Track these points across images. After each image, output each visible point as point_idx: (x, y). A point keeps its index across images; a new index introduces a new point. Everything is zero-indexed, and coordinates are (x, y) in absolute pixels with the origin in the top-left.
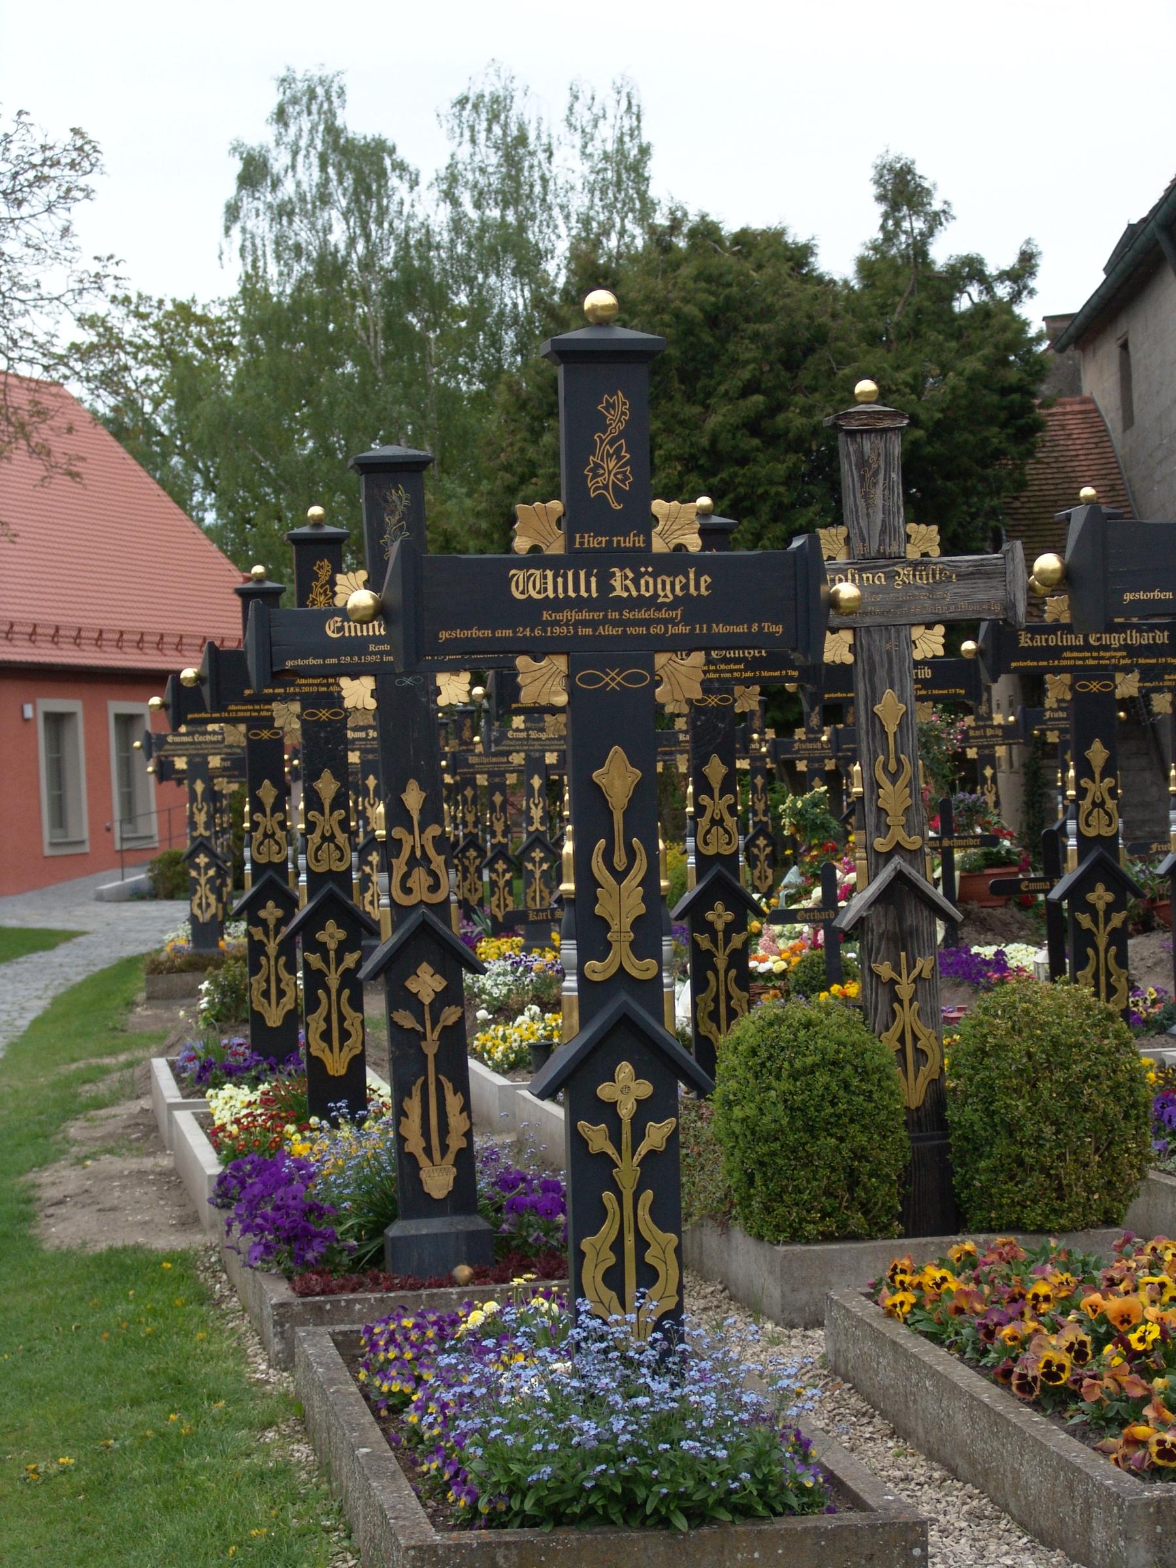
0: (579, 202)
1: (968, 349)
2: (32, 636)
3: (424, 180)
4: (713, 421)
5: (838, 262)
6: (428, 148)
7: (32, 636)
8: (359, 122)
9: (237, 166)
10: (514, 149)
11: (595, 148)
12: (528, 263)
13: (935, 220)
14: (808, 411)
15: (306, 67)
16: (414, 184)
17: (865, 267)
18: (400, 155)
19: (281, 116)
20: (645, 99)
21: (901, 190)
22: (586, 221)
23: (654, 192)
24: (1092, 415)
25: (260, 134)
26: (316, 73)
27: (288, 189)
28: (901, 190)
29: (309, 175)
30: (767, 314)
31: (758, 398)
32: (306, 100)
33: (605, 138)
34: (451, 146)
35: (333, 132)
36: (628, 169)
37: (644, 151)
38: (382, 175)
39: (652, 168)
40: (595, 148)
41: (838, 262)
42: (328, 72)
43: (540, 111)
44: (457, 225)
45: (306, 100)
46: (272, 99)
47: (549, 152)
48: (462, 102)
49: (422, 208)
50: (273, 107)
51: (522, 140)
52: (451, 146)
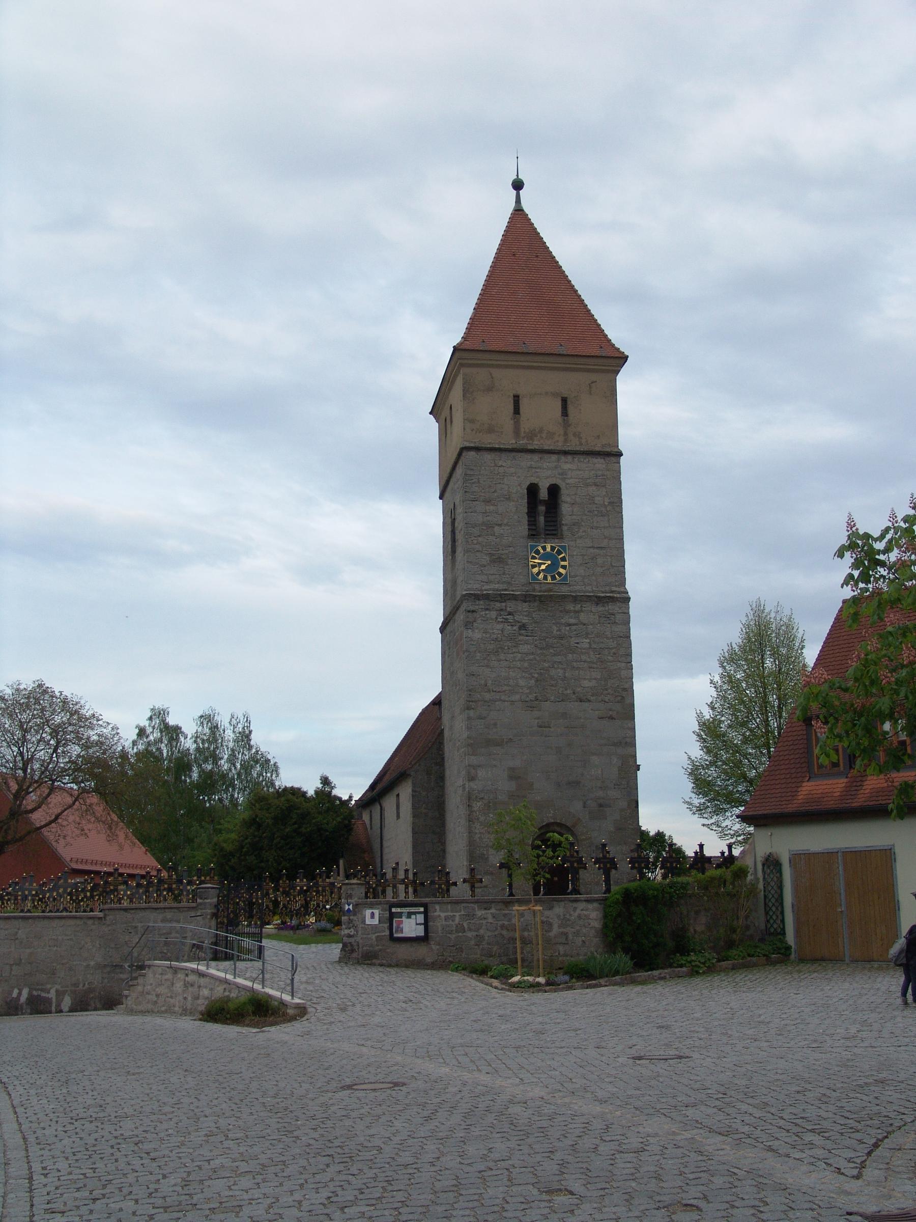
0: (231, 745)
1: (338, 816)
2: (77, 862)
3: (189, 736)
4: (287, 830)
5: (311, 792)
6: (190, 727)
7: (77, 862)
8: (172, 721)
9: (137, 731)
10: (214, 728)
11: (237, 730)
12: (216, 759)
13: (332, 788)
14: (306, 828)
15: (159, 705)
16: (186, 738)
17: (316, 792)
18: (183, 729)
19: (151, 719)
20: (252, 719)
21: (325, 781)
22: (233, 750)
23: (252, 743)
24: (364, 824)
25: (144, 723)
26: (161, 707)
27: (151, 738)
28: (325, 781)
29: (157, 734)
30: (298, 808)
31: (296, 826)
32: (159, 715)
33: (240, 728)
34: (196, 728)
35: (163, 721)
36: (245, 737)
37: (250, 732)
38: (177, 735)
39: (253, 736)
40: (237, 730)
41: (311, 792)
42: (165, 707)
43: (223, 720)
44: (198, 749)
45: (159, 715)
46: (149, 714)
47: (224, 731)
48: (201, 717)
49: (188, 744)
50: (149, 715)
51: (217, 727)
52: (196, 728)
